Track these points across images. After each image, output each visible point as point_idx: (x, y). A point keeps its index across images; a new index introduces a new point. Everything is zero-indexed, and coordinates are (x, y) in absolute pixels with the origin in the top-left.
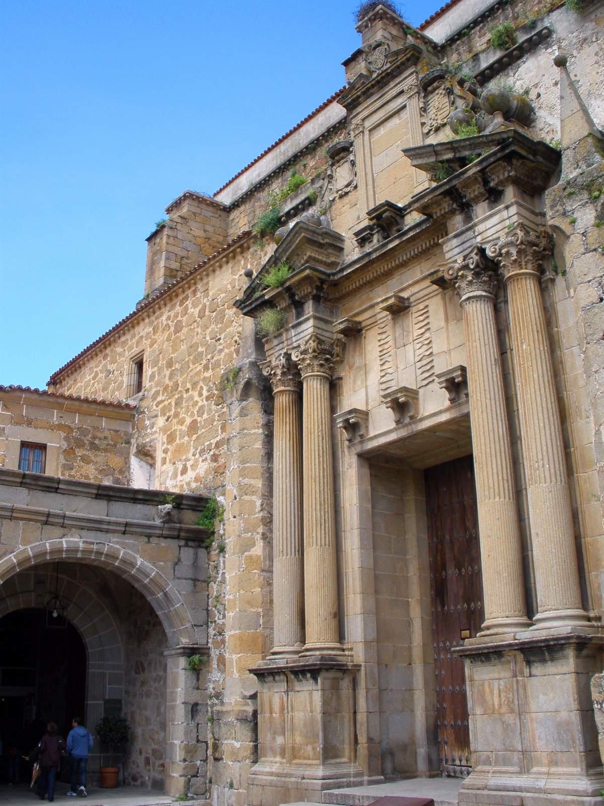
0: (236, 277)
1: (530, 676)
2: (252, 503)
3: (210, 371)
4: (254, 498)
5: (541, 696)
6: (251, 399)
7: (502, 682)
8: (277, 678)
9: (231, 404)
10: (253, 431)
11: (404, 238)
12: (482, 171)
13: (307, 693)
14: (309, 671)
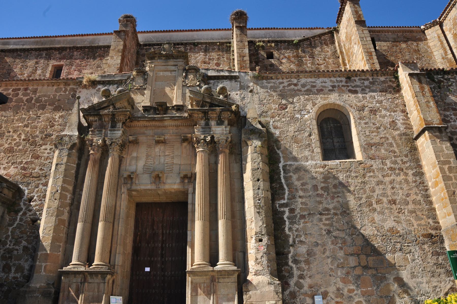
0: (58, 94)
1: (218, 282)
2: (66, 196)
3: (29, 128)
4: (67, 194)
5: (222, 289)
6: (74, 151)
7: (205, 284)
9: (62, 149)
10: (72, 165)
13: (96, 284)
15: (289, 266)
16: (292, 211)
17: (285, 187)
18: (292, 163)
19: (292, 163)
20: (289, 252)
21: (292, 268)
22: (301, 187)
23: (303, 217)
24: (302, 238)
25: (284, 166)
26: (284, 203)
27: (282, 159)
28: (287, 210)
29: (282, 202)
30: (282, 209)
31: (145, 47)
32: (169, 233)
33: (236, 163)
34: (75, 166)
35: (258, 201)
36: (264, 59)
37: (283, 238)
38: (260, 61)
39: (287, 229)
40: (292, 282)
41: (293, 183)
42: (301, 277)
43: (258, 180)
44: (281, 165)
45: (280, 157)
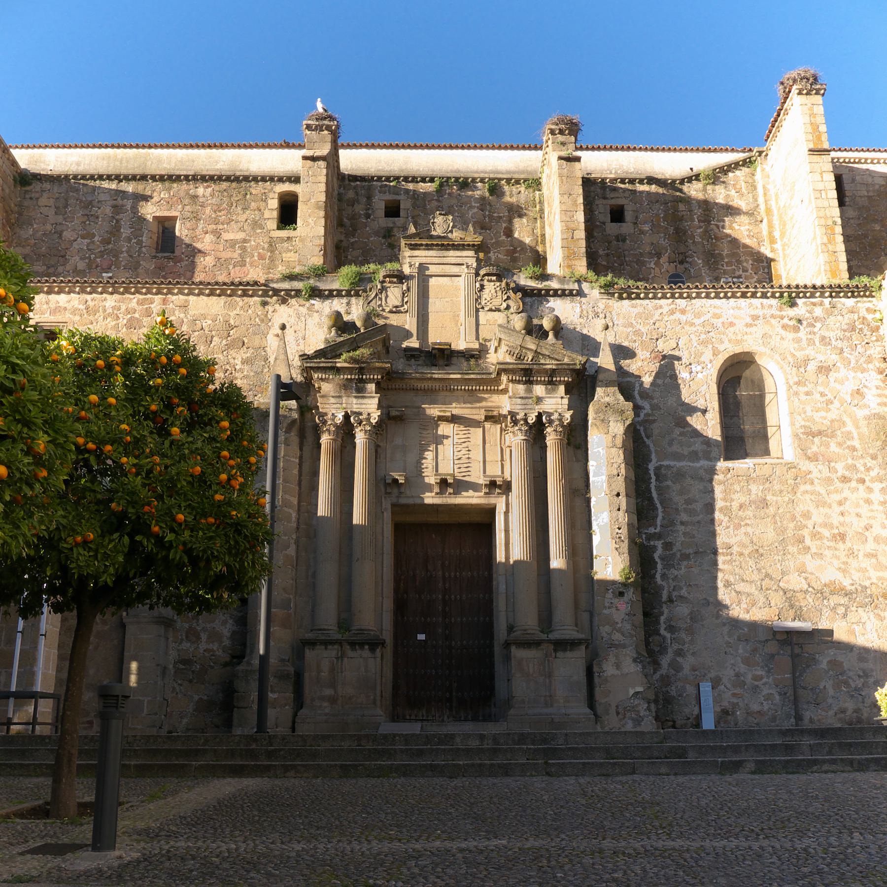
4: (291, 511)
8: (330, 647)
11: (466, 377)
12: (554, 370)
14: (368, 644)
15: (660, 635)
16: (668, 546)
17: (659, 506)
18: (672, 463)
19: (672, 463)
20: (662, 614)
21: (664, 638)
22: (684, 506)
23: (686, 557)
24: (684, 592)
25: (658, 469)
26: (655, 533)
27: (653, 456)
28: (659, 544)
29: (652, 530)
30: (652, 543)
31: (352, 184)
32: (455, 576)
33: (578, 461)
34: (297, 461)
35: (617, 530)
36: (604, 223)
37: (652, 591)
38: (597, 226)
39: (658, 576)
40: (665, 661)
41: (671, 499)
42: (679, 653)
43: (618, 495)
44: (651, 467)
45: (650, 451)
